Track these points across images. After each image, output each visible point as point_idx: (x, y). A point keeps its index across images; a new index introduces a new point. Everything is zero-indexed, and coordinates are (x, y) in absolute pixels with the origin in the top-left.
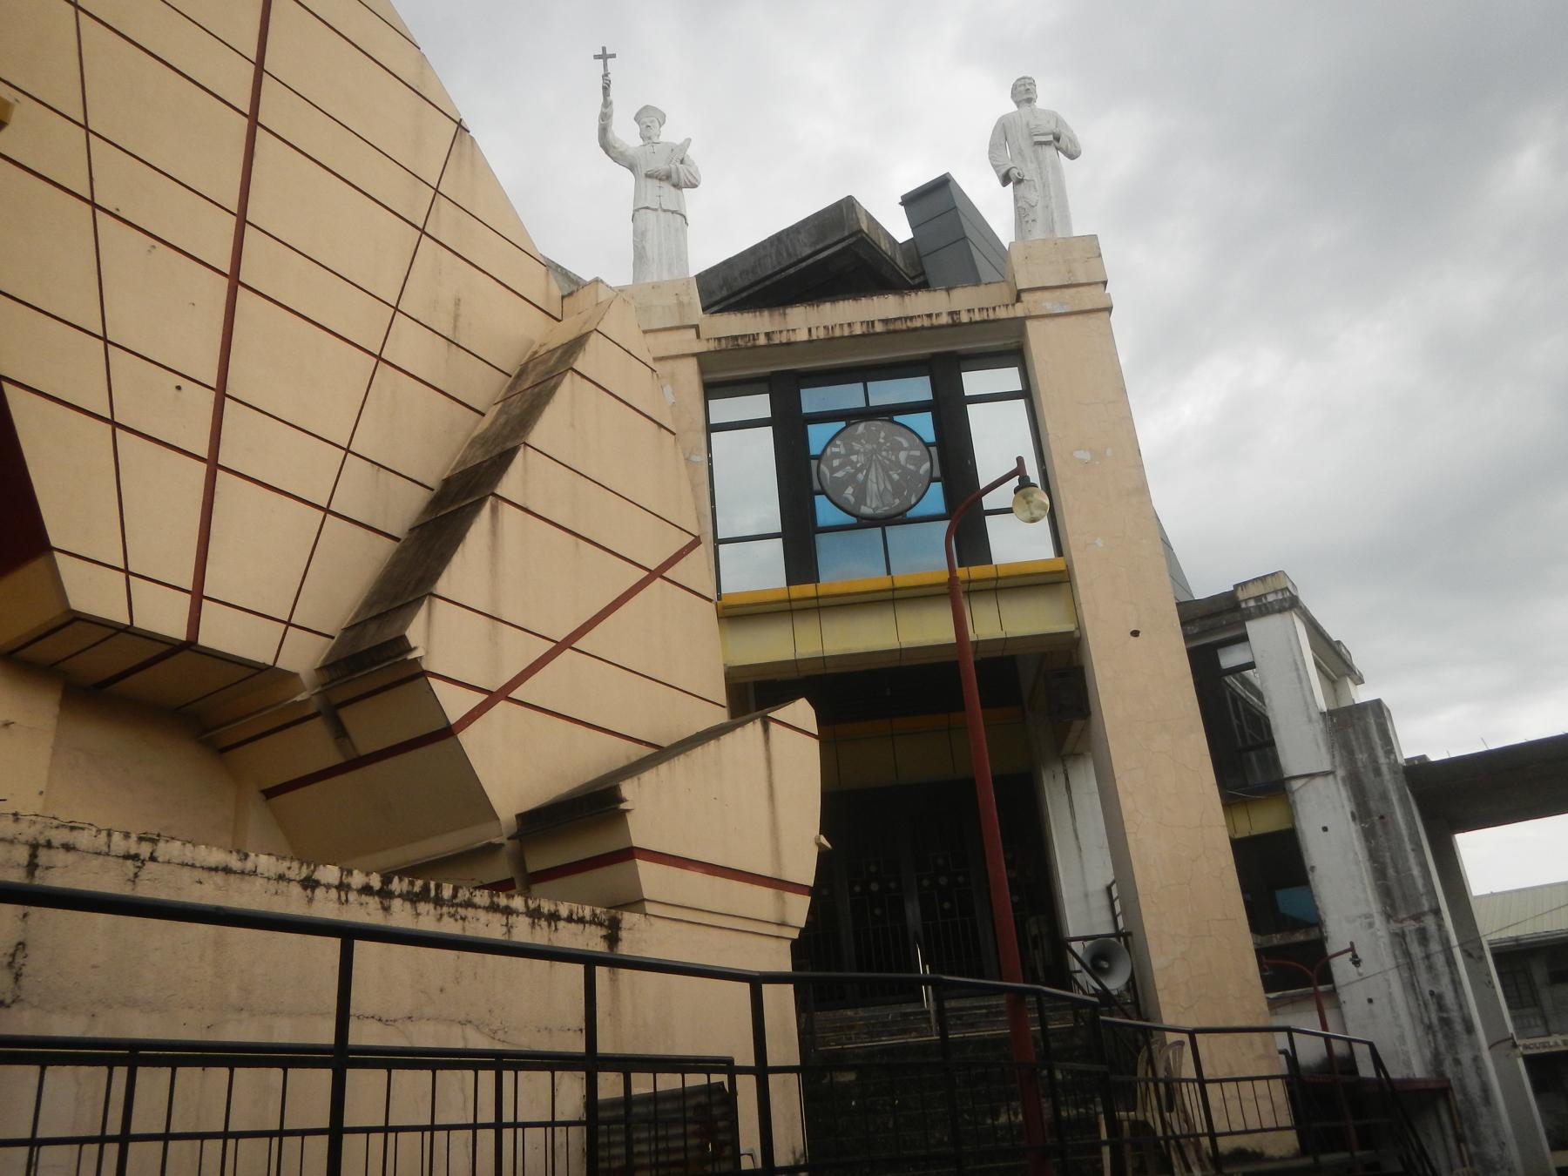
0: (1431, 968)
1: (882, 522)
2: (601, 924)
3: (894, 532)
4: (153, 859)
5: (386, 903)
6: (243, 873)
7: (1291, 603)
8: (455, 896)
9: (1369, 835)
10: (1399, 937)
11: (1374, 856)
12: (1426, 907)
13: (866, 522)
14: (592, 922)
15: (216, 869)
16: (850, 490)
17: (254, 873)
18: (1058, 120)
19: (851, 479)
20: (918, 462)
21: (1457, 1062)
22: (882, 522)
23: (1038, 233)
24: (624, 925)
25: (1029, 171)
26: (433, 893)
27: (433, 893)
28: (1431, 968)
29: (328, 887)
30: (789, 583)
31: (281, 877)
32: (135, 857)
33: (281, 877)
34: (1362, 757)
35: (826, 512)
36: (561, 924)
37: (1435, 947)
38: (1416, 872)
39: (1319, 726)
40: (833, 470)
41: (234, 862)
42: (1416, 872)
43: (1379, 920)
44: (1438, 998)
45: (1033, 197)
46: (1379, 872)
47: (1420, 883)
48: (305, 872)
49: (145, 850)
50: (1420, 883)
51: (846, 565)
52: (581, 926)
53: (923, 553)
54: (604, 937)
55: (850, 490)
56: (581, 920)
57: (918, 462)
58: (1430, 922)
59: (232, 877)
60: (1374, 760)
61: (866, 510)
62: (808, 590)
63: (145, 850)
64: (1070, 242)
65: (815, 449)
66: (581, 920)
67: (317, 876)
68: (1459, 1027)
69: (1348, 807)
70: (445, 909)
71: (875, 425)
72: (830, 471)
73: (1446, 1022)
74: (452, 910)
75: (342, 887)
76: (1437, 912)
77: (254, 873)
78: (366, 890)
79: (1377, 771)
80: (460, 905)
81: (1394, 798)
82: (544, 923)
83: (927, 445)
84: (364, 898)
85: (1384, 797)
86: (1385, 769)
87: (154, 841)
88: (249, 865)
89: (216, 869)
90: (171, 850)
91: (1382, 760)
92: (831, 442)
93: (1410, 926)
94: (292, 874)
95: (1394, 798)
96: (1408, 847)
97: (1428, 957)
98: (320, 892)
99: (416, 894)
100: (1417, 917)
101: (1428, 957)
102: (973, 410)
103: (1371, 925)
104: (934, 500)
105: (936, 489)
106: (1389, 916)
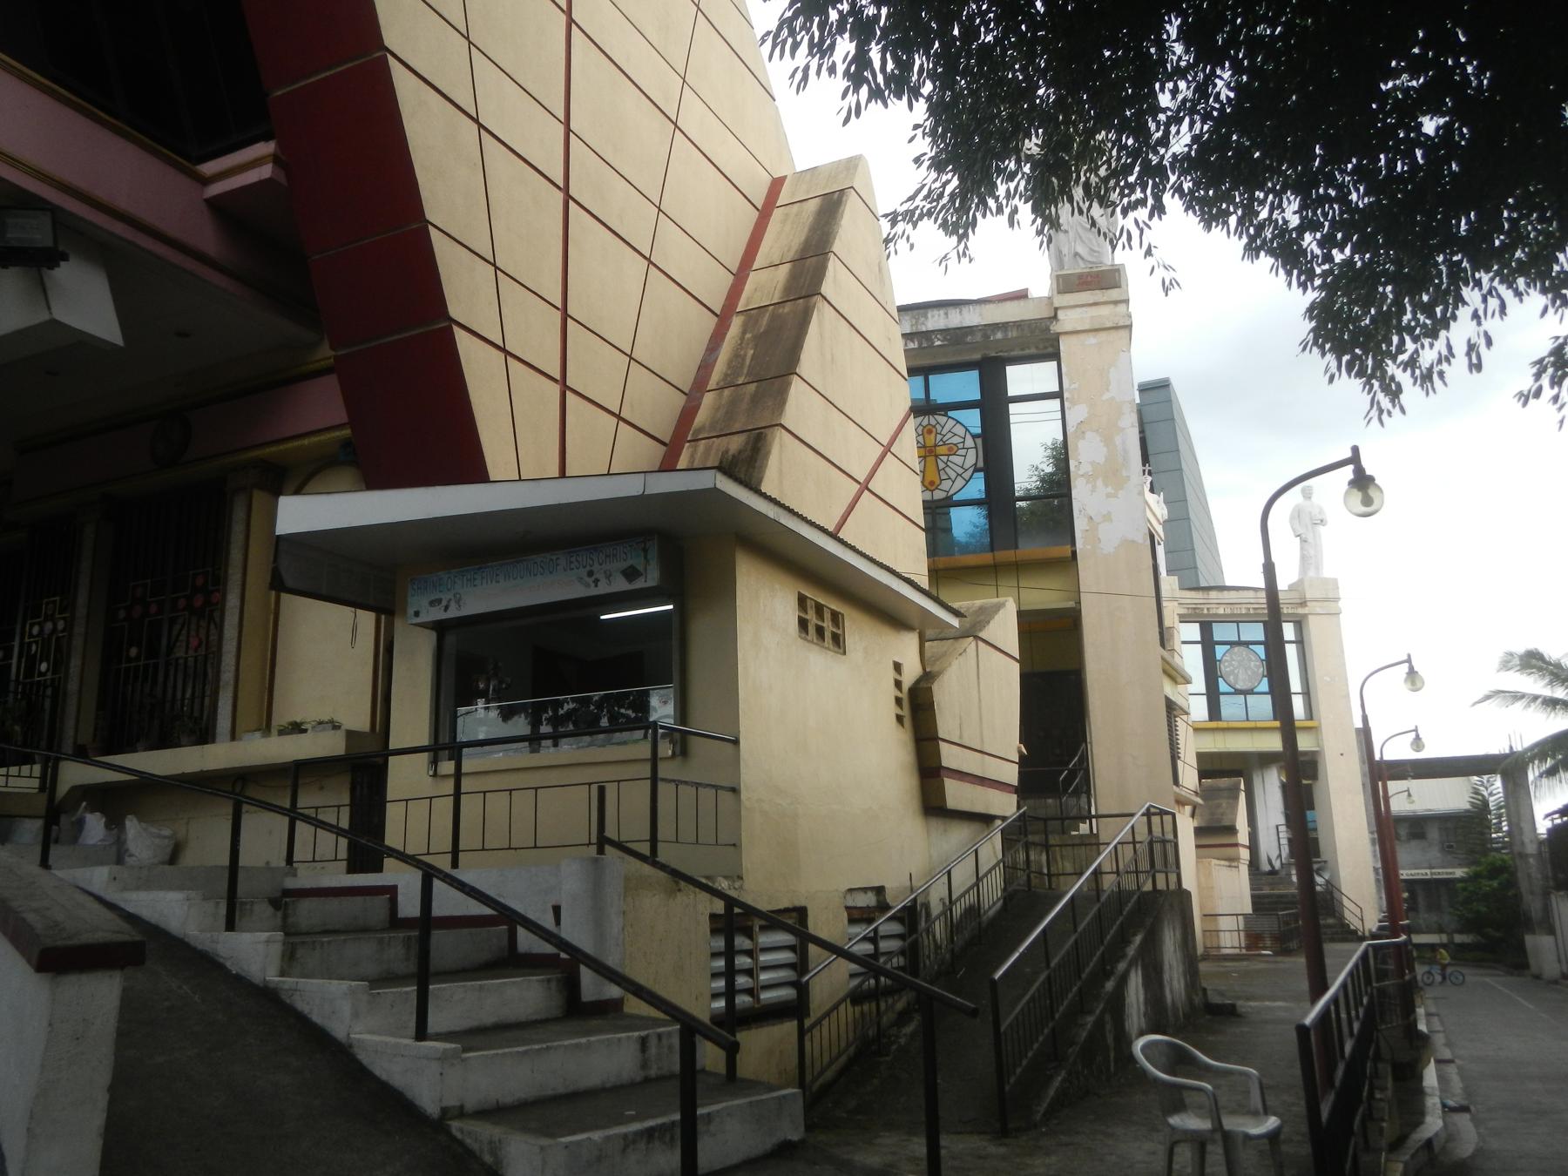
1: (1245, 693)
13: (1238, 692)
18: (1321, 511)
19: (1232, 672)
22: (1245, 693)
23: (1311, 573)
25: (1310, 540)
35: (1223, 687)
45: (1312, 552)
51: (1231, 707)
53: (1262, 706)
64: (1326, 581)
71: (1242, 648)
72: (1224, 668)
105: (1265, 680)
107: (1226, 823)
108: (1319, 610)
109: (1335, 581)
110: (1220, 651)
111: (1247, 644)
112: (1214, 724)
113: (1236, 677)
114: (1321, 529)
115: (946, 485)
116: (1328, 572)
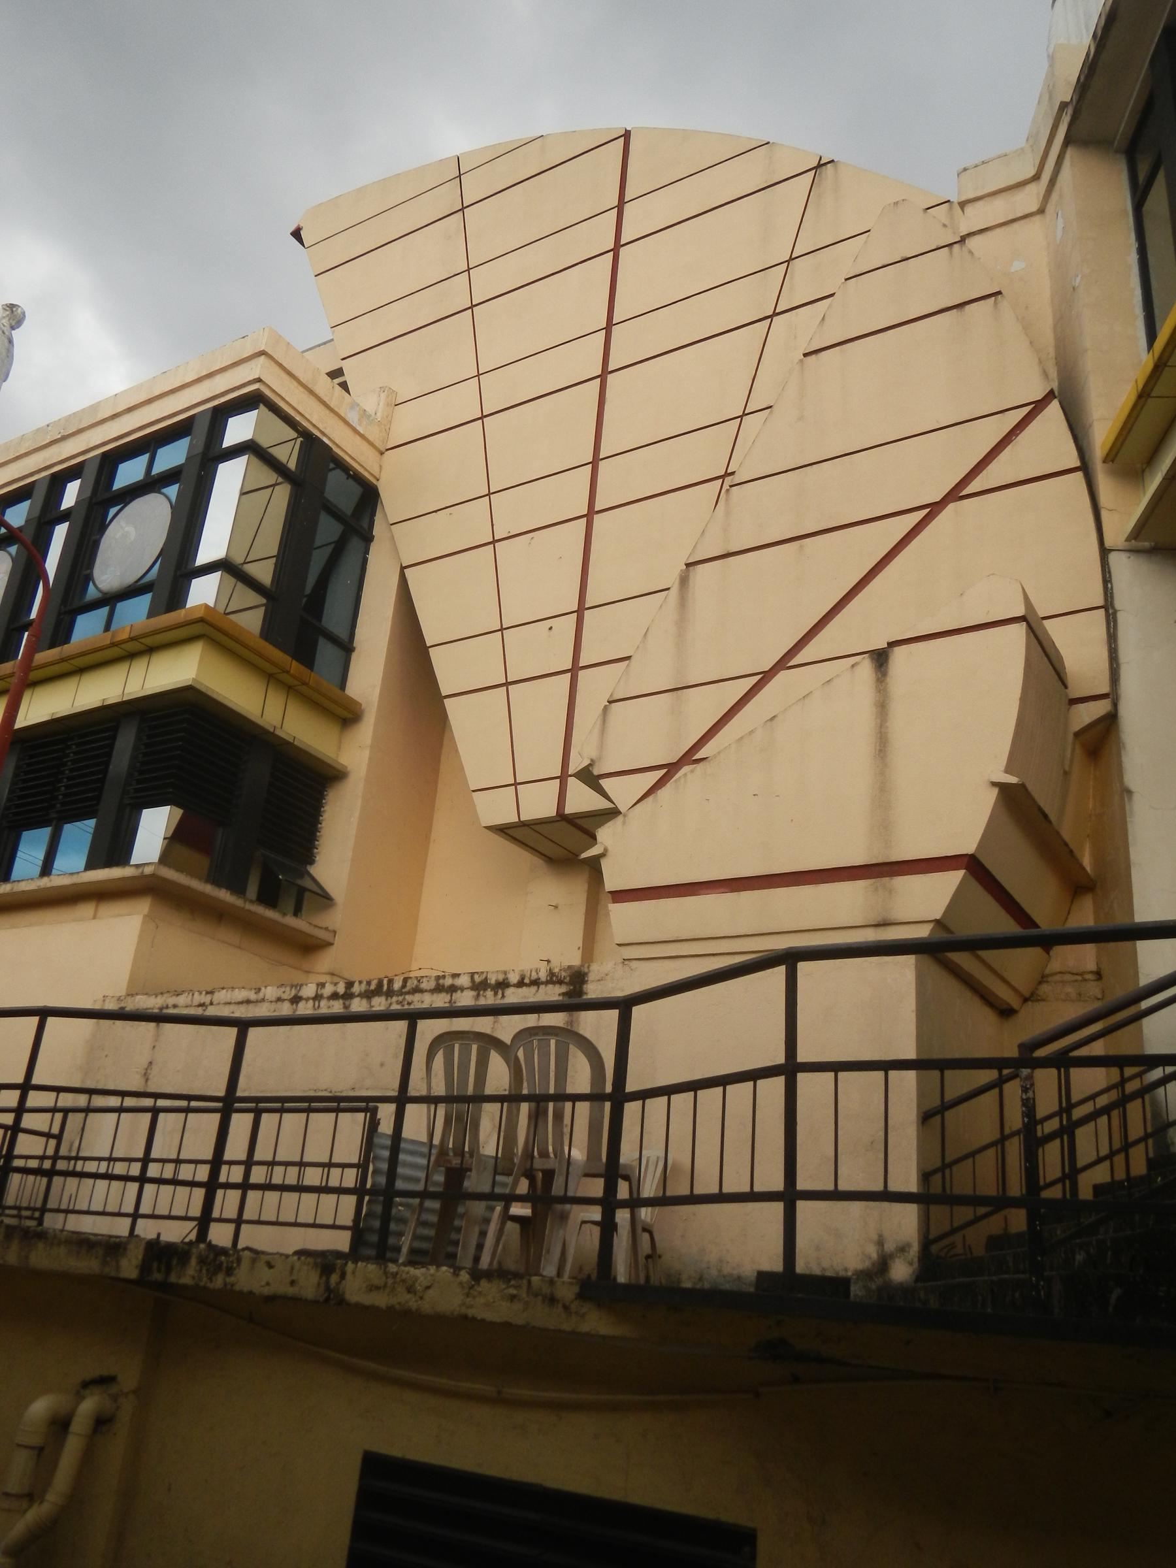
2: (560, 982)
4: (211, 1004)
5: (347, 1003)
6: (257, 1001)
8: (404, 986)
14: (547, 983)
15: (241, 1003)
17: (263, 1000)
24: (591, 977)
26: (385, 987)
27: (385, 987)
29: (307, 999)
31: (279, 1000)
32: (201, 1005)
33: (279, 1000)
36: (510, 991)
41: (252, 996)
48: (293, 992)
49: (207, 999)
52: (533, 989)
54: (563, 994)
56: (536, 983)
59: (251, 1005)
63: (207, 999)
66: (536, 983)
67: (300, 994)
70: (395, 999)
74: (400, 998)
75: (317, 997)
77: (263, 1000)
78: (335, 996)
80: (408, 993)
82: (489, 993)
84: (332, 1002)
87: (211, 992)
88: (261, 995)
89: (241, 1003)
90: (221, 996)
94: (285, 996)
98: (301, 1004)
99: (372, 991)
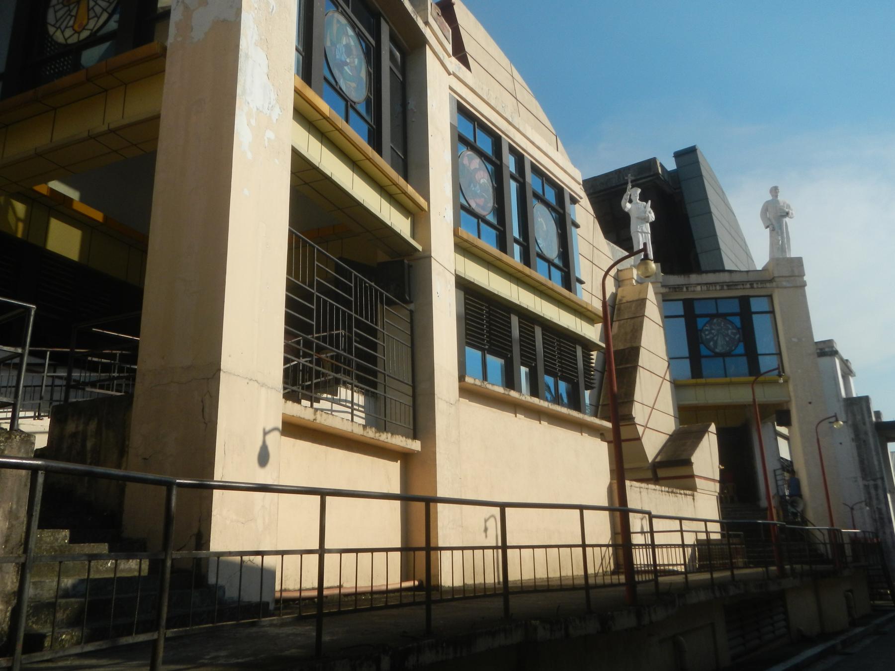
0: (878, 499)
1: (723, 355)
3: (728, 360)
7: (835, 353)
9: (859, 448)
10: (867, 487)
11: (860, 455)
12: (878, 475)
13: (717, 355)
16: (712, 343)
19: (712, 339)
20: (735, 334)
21: (884, 533)
22: (723, 355)
28: (878, 499)
30: (693, 377)
34: (859, 417)
35: (704, 351)
37: (880, 492)
38: (876, 463)
39: (842, 404)
40: (706, 335)
42: (876, 463)
43: (860, 479)
44: (880, 510)
46: (861, 462)
47: (877, 468)
50: (877, 468)
55: (712, 343)
57: (735, 334)
58: (879, 482)
60: (863, 419)
61: (717, 351)
62: (699, 381)
64: (792, 260)
65: (700, 326)
68: (886, 520)
69: (852, 436)
73: (882, 519)
76: (882, 478)
79: (864, 424)
81: (870, 434)
83: (738, 329)
85: (866, 433)
86: (868, 424)
91: (867, 419)
92: (705, 325)
93: (871, 483)
95: (870, 434)
96: (874, 453)
97: (877, 495)
100: (875, 480)
101: (877, 495)
102: (754, 317)
103: (856, 481)
104: (741, 349)
106: (864, 478)
107: (684, 457)
108: (785, 284)
109: (800, 260)
110: (701, 322)
111: (724, 316)
112: (694, 381)
113: (716, 343)
114: (787, 219)
115: (91, 25)
116: (794, 253)
